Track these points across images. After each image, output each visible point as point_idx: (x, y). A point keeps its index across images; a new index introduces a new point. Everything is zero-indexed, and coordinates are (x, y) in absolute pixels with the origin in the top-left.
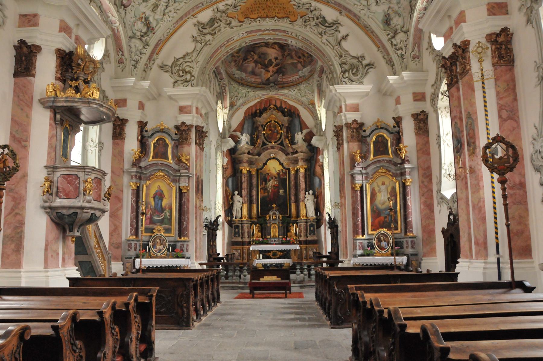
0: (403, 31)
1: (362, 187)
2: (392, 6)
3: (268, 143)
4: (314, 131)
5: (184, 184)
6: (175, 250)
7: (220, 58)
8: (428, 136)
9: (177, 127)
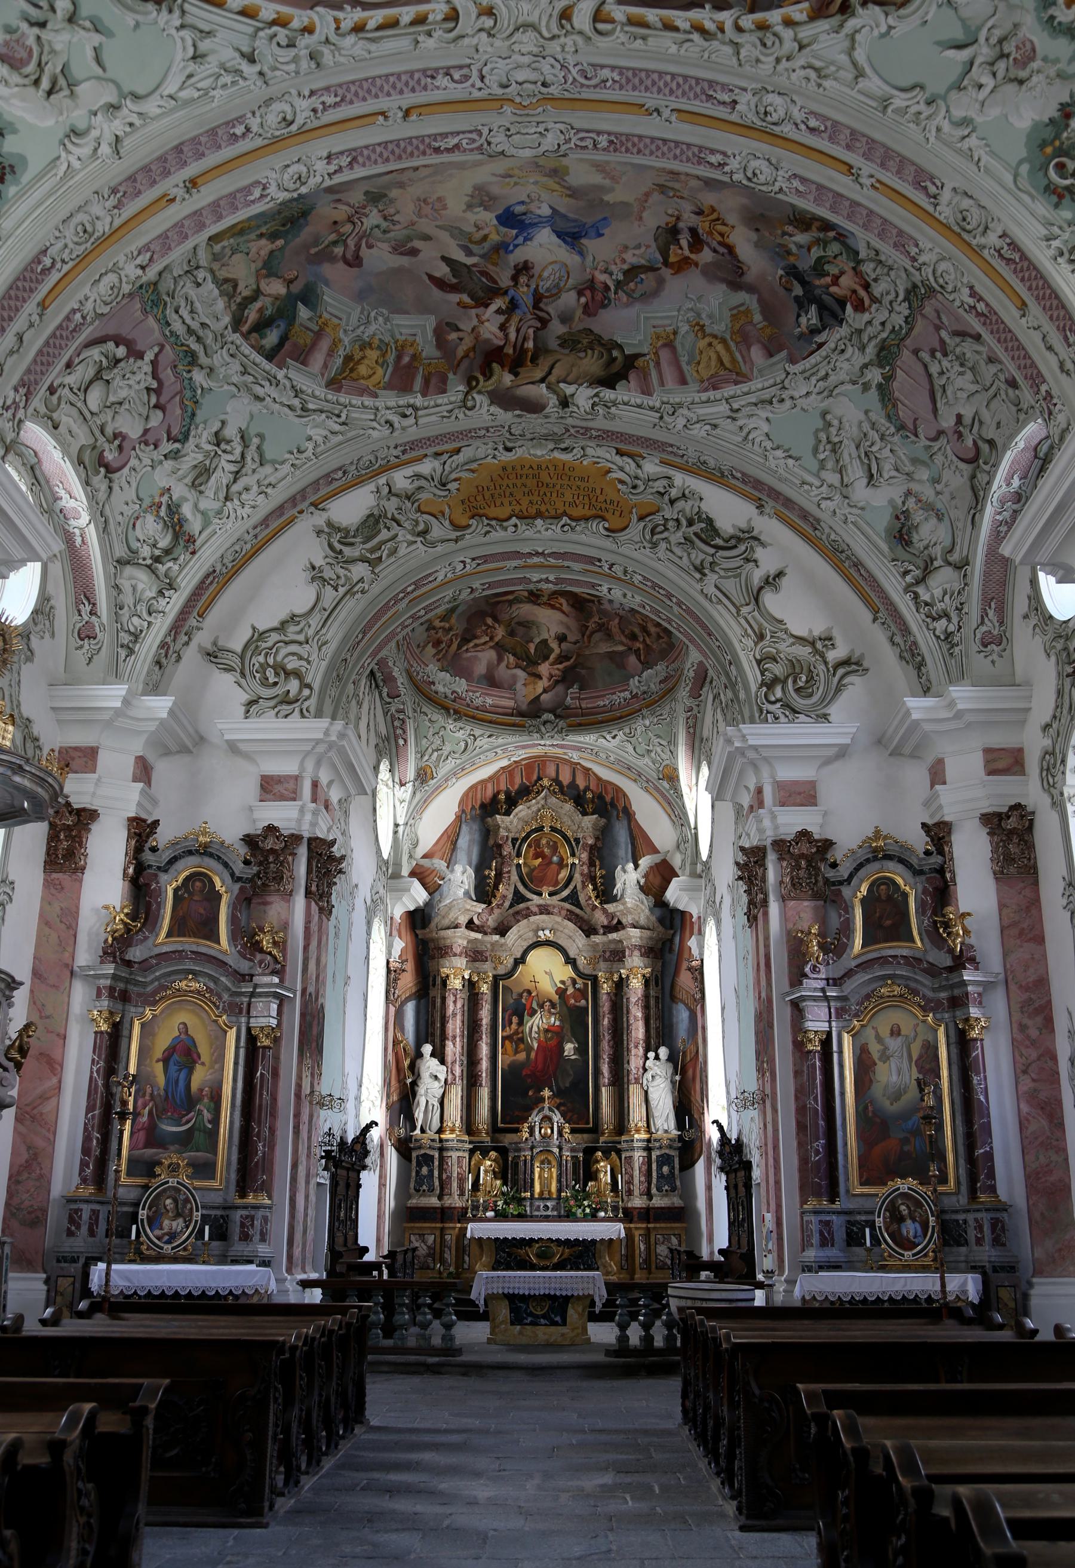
0: (949, 564)
1: (826, 1043)
2: (915, 487)
3: (529, 895)
4: (676, 861)
5: (263, 1021)
6: (223, 1235)
7: (393, 634)
9: (249, 840)
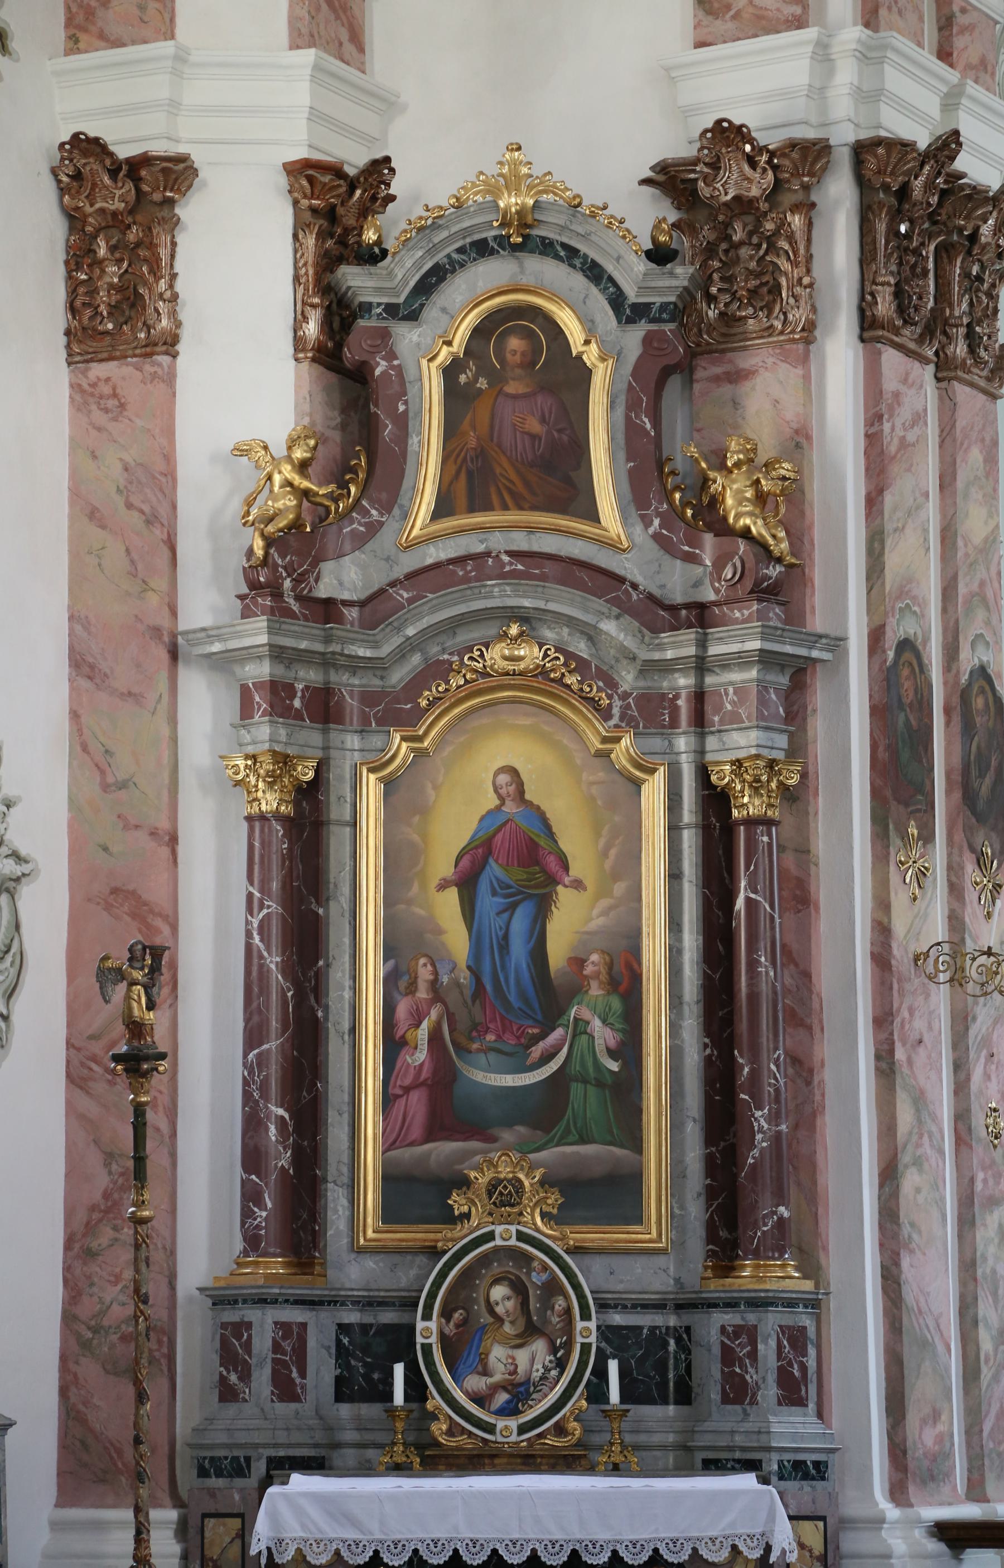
9: (670, 180)
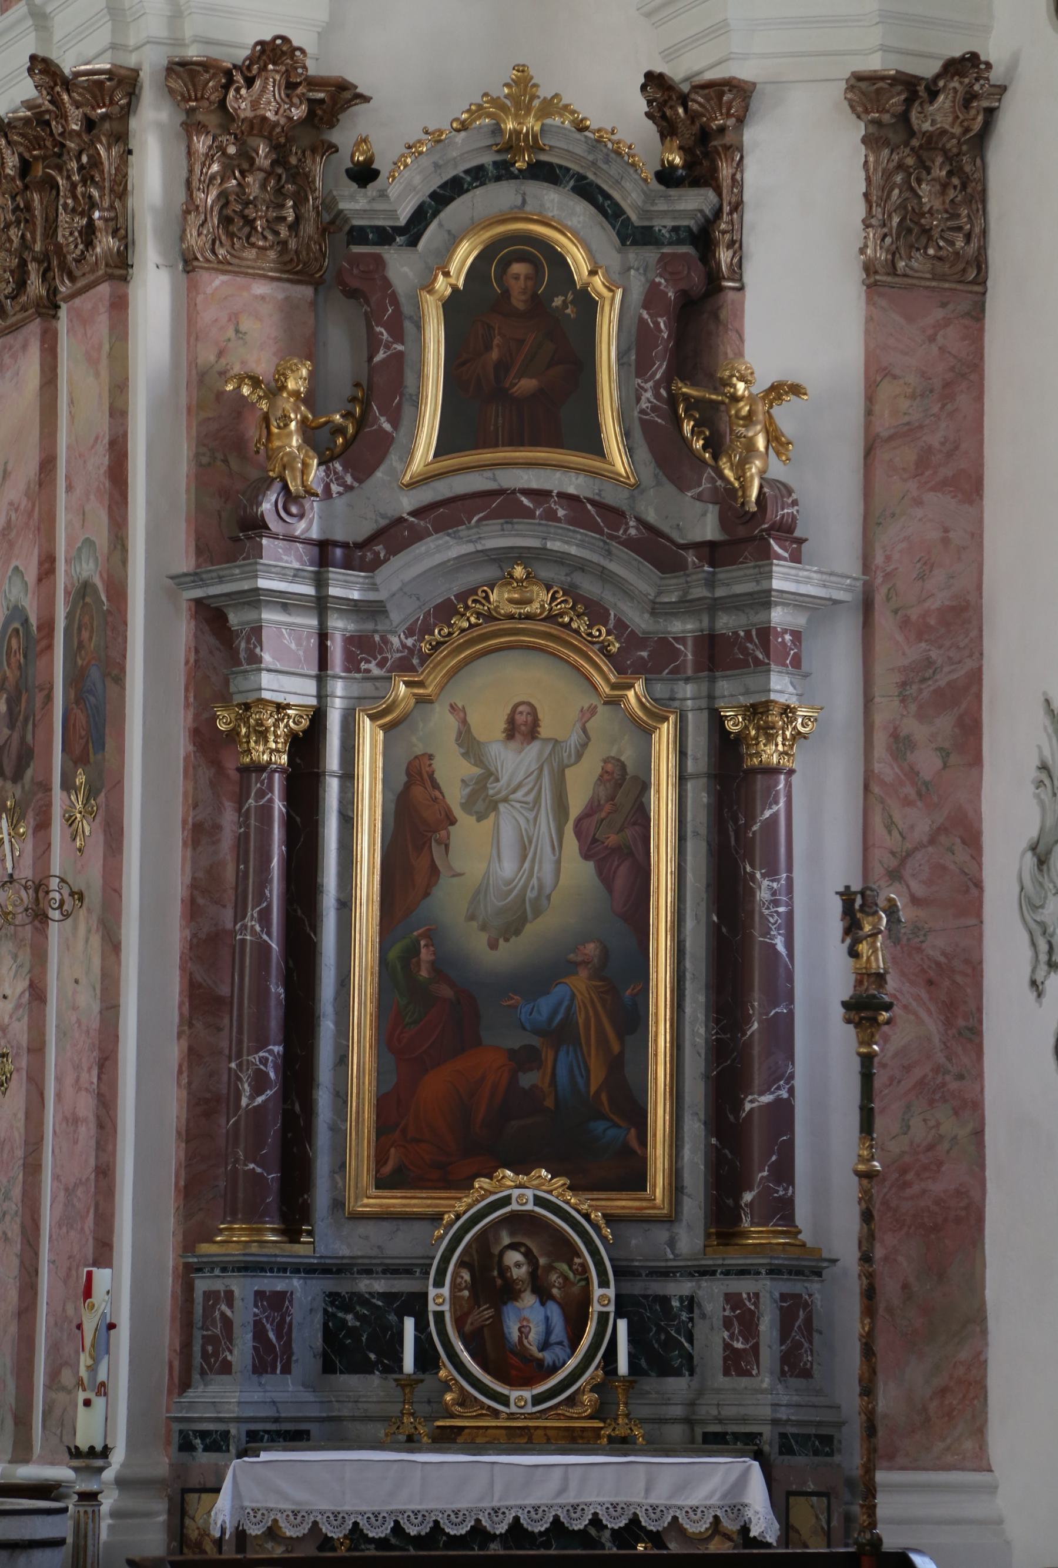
1: (307, 744)
8: (977, 313)
